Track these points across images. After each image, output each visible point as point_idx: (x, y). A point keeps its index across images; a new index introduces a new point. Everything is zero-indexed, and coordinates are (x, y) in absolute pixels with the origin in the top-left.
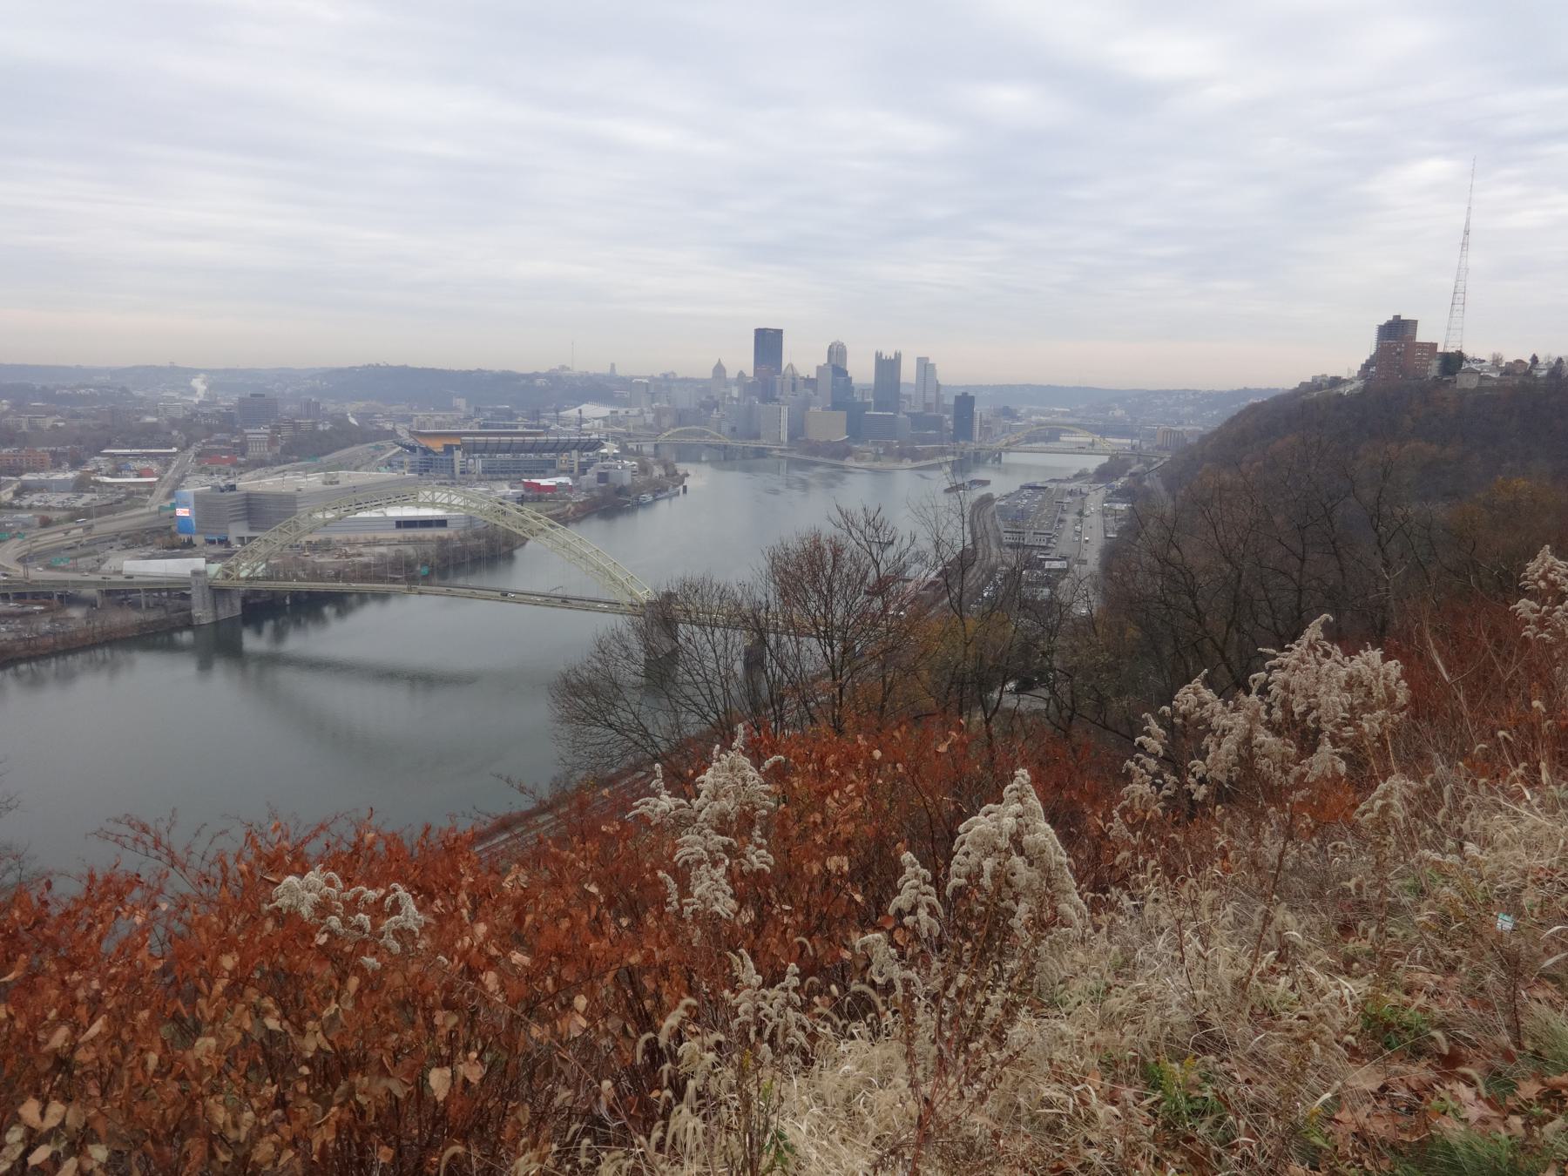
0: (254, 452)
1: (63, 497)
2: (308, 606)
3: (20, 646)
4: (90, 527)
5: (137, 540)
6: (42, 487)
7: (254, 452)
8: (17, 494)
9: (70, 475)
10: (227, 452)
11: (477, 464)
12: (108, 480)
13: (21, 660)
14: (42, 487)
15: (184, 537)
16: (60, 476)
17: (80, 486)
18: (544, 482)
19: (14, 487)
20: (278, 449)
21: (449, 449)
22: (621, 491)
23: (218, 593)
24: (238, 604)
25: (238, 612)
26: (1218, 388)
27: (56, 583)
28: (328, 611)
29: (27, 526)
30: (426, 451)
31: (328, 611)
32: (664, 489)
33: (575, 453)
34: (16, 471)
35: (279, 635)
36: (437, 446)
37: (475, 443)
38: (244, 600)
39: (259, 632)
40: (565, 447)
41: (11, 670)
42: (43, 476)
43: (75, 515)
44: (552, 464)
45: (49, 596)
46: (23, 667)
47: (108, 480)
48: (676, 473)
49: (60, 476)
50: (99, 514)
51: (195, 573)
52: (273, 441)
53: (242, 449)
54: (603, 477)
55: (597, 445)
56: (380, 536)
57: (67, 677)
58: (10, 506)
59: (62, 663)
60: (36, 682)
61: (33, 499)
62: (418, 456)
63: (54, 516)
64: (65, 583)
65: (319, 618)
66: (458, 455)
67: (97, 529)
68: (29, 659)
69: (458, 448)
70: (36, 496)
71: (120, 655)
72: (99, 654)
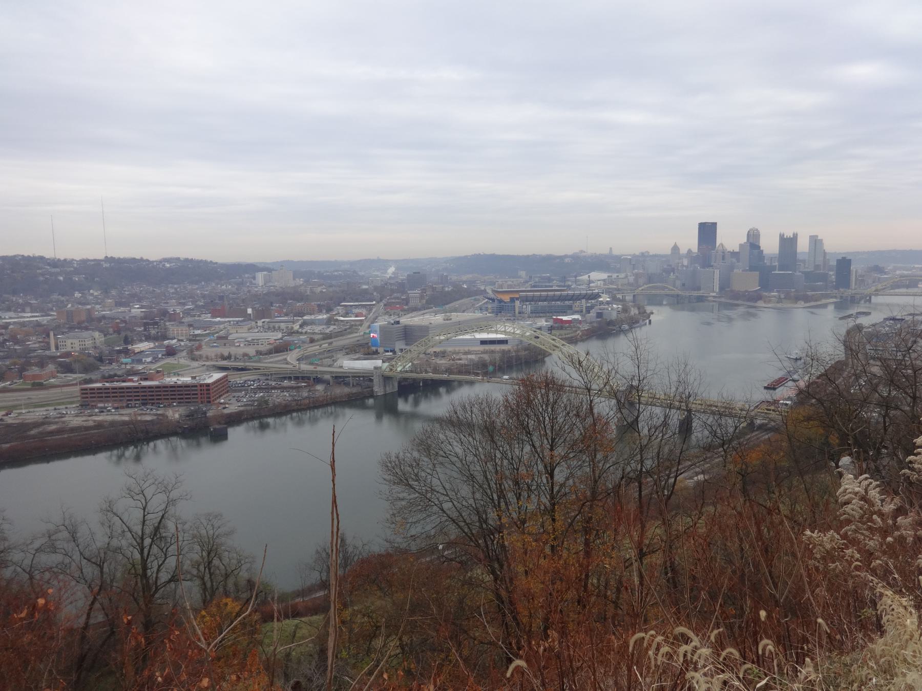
0: (412, 303)
1: (320, 328)
2: (431, 387)
3: (294, 404)
5: (353, 350)
6: (312, 323)
7: (412, 303)
8: (301, 326)
9: (325, 316)
10: (398, 303)
11: (528, 308)
12: (342, 319)
13: (294, 411)
14: (312, 323)
15: (374, 349)
16: (320, 317)
17: (329, 322)
18: (565, 318)
19: (300, 322)
20: (424, 301)
21: (513, 300)
22: (611, 323)
23: (387, 379)
24: (396, 385)
25: (396, 389)
28: (442, 390)
29: (304, 342)
30: (500, 301)
31: (442, 390)
32: (637, 322)
33: (584, 301)
34: (301, 314)
35: (416, 403)
36: (506, 298)
37: (527, 296)
38: (399, 383)
39: (406, 400)
40: (578, 298)
41: (289, 416)
42: (313, 317)
43: (327, 337)
44: (570, 307)
45: (309, 378)
46: (294, 414)
47: (342, 319)
48: (645, 312)
50: (337, 336)
51: (376, 368)
52: (422, 297)
53: (407, 301)
54: (599, 315)
55: (597, 296)
58: (297, 332)
59: (312, 413)
60: (300, 423)
61: (307, 329)
62: (496, 304)
63: (316, 337)
65: (438, 394)
66: (517, 303)
67: (335, 344)
68: (297, 411)
69: (517, 299)
70: (309, 327)
71: (339, 410)
72: (329, 409)
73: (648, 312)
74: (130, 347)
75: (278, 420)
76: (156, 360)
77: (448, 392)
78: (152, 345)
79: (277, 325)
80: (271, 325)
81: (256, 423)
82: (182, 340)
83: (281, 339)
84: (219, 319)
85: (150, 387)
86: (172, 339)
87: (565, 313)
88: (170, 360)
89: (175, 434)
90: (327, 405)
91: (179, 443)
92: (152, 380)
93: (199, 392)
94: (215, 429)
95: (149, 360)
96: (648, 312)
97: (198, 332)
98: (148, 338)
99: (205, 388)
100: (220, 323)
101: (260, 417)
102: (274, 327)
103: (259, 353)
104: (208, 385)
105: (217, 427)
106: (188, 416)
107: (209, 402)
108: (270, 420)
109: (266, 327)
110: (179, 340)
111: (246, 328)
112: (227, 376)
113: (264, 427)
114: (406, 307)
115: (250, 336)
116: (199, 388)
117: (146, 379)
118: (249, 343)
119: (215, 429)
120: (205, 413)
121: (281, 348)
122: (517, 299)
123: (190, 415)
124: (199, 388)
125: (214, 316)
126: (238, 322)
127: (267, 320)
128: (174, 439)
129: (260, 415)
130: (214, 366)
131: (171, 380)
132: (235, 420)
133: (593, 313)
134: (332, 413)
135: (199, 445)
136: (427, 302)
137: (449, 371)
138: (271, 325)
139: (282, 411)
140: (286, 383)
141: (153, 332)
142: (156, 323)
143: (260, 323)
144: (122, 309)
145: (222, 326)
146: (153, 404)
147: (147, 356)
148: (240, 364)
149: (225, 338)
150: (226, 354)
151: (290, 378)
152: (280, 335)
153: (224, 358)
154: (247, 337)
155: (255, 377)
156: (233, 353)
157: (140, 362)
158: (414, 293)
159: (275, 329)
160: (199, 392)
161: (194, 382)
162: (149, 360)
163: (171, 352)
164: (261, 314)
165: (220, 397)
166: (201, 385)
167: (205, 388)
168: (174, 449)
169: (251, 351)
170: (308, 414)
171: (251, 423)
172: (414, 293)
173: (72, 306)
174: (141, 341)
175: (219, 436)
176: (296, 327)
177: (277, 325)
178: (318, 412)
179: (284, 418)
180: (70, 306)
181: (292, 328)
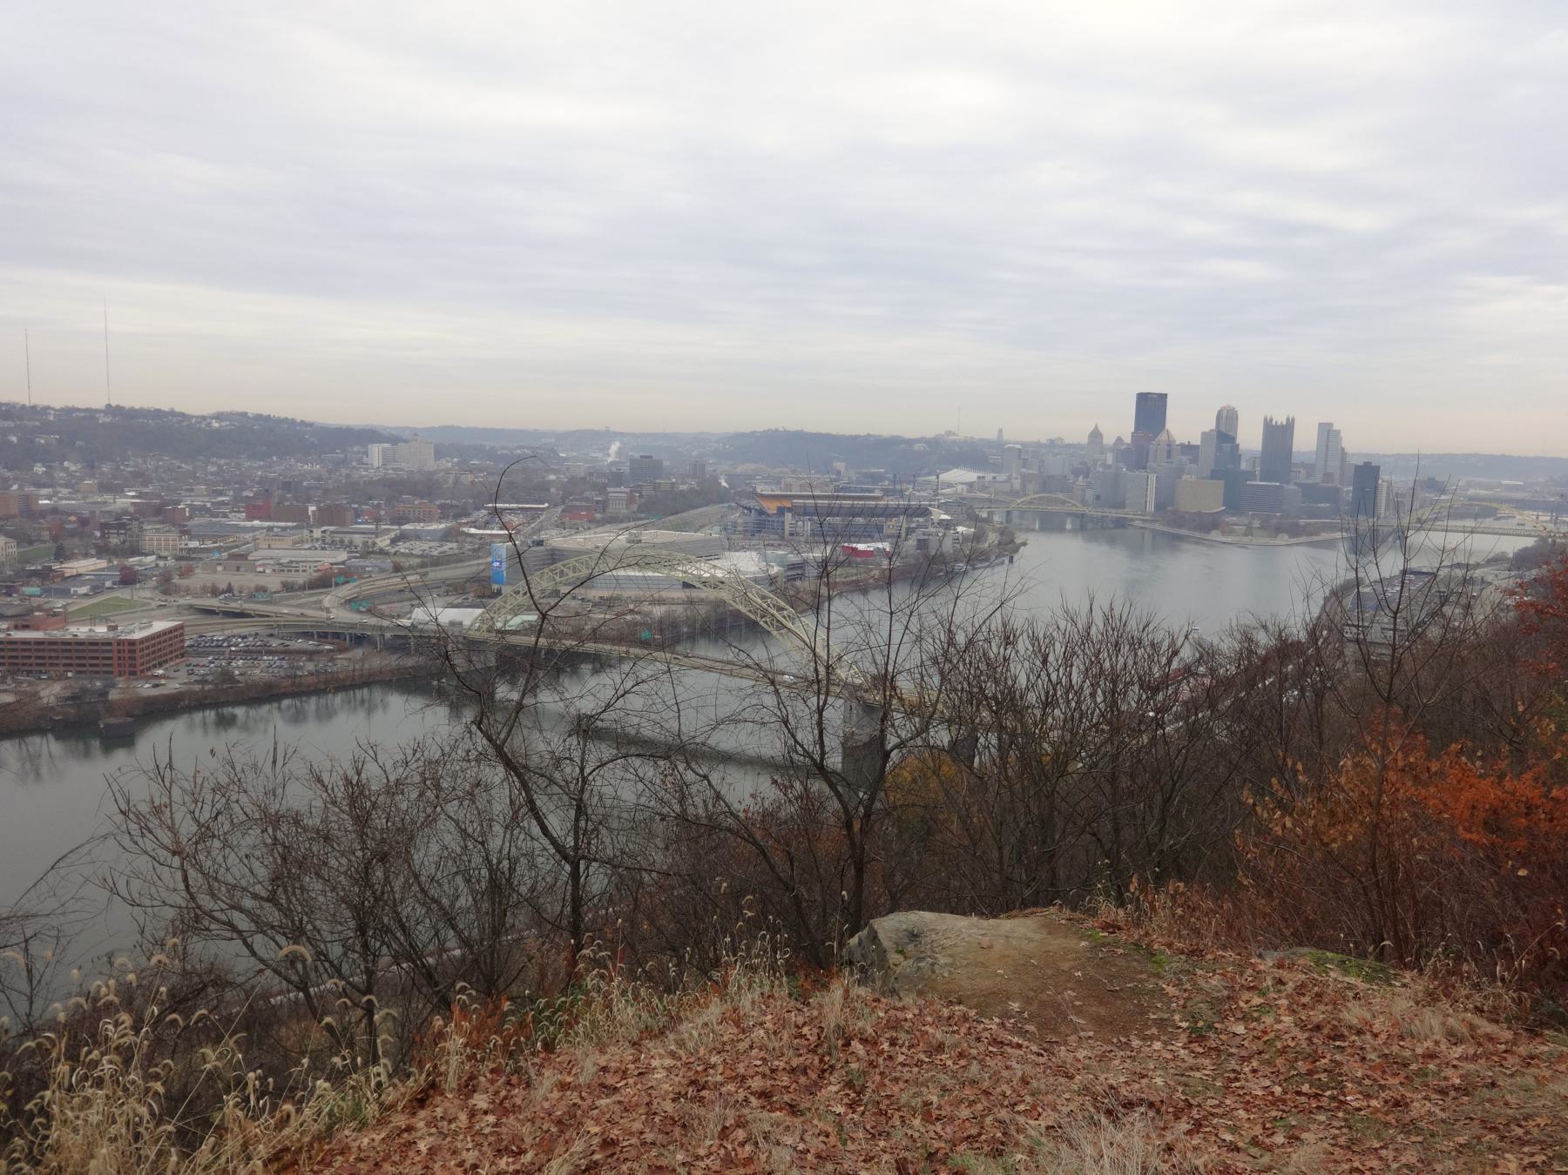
0: (611, 510)
1: (425, 546)
4: (425, 574)
5: (458, 591)
6: (417, 536)
8: (393, 542)
9: (442, 526)
10: (581, 508)
11: (807, 526)
12: (473, 531)
13: (285, 695)
14: (417, 536)
15: (495, 587)
16: (434, 526)
17: (447, 536)
18: (861, 547)
19: (392, 535)
20: (635, 507)
21: (781, 511)
23: (473, 646)
25: (492, 662)
26: (464, 423)
27: (353, 626)
29: (382, 570)
30: (761, 512)
31: (586, 668)
32: (987, 560)
34: (400, 520)
36: (771, 508)
37: (805, 506)
39: (512, 683)
42: (419, 526)
43: (437, 562)
44: (880, 529)
45: (336, 635)
46: (286, 702)
47: (473, 531)
48: (1012, 541)
49: (434, 526)
51: (452, 624)
52: (631, 500)
53: (604, 505)
54: (922, 544)
55: (924, 512)
56: (664, 594)
57: (326, 715)
58: (382, 552)
59: (322, 701)
60: (298, 717)
61: (402, 547)
63: (405, 562)
64: (364, 626)
65: (575, 671)
66: (788, 516)
67: (432, 576)
68: (293, 695)
69: (790, 510)
71: (377, 694)
73: (1018, 541)
74: (56, 567)
75: (252, 712)
76: (97, 589)
77: (595, 672)
78: (103, 563)
79: (347, 538)
80: (337, 537)
81: (210, 715)
82: (165, 558)
83: (343, 563)
84: (256, 523)
85: (25, 642)
86: (146, 555)
87: (867, 536)
88: (124, 593)
89: (40, 731)
90: (360, 686)
91: (48, 746)
92: (37, 629)
93: (115, 655)
94: (107, 725)
95: (84, 590)
96: (1018, 541)
97: (194, 544)
98: (103, 551)
99: (126, 648)
100: (253, 529)
101: (216, 705)
102: (342, 542)
103: (288, 587)
104: (132, 643)
105: (113, 721)
106: (72, 698)
107: (133, 673)
108: (240, 711)
109: (328, 540)
110: (160, 557)
111: (288, 541)
112: (181, 627)
113: (225, 722)
114: (598, 516)
115: (286, 556)
116: (115, 647)
117: (26, 627)
118: (282, 567)
119: (107, 725)
120: (103, 694)
121: (323, 582)
122: (790, 510)
123: (75, 698)
124: (115, 647)
125: (250, 518)
126: (284, 529)
127: (332, 528)
128: (35, 742)
129: (222, 699)
130: (191, 607)
131: (81, 631)
132: (168, 708)
133: (912, 542)
134: (363, 701)
135: (87, 754)
136: (640, 510)
137: (595, 636)
138: (337, 537)
139: (266, 694)
140: (300, 644)
141: (114, 541)
142: (122, 526)
143: (317, 533)
144: (108, 497)
145: (248, 536)
146: (29, 673)
147: (83, 584)
148: (235, 606)
149: (244, 557)
150: (223, 586)
151: (307, 635)
152: (342, 556)
153: (215, 592)
154: (281, 553)
155: (253, 630)
156: (235, 585)
157: (65, 593)
158: (618, 493)
159: (342, 545)
160: (115, 655)
161: (111, 635)
162: (84, 590)
163: (129, 579)
164: (330, 515)
165: (160, 665)
166: (119, 643)
167: (126, 648)
168: (33, 759)
169: (273, 582)
170: (312, 704)
171: (198, 716)
172: (618, 493)
173: (21, 487)
174: (86, 556)
175: (120, 738)
176: (383, 542)
177: (347, 538)
178: (338, 699)
179: (266, 708)
180: (15, 487)
181: (374, 544)
